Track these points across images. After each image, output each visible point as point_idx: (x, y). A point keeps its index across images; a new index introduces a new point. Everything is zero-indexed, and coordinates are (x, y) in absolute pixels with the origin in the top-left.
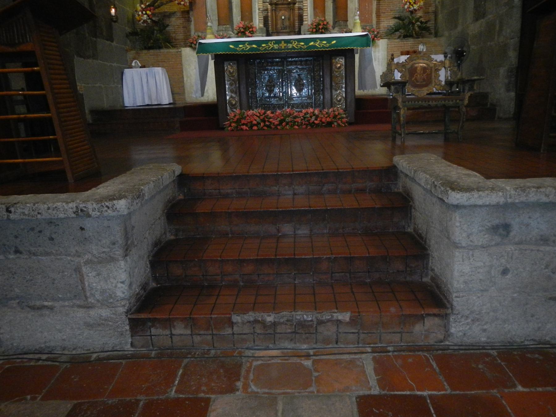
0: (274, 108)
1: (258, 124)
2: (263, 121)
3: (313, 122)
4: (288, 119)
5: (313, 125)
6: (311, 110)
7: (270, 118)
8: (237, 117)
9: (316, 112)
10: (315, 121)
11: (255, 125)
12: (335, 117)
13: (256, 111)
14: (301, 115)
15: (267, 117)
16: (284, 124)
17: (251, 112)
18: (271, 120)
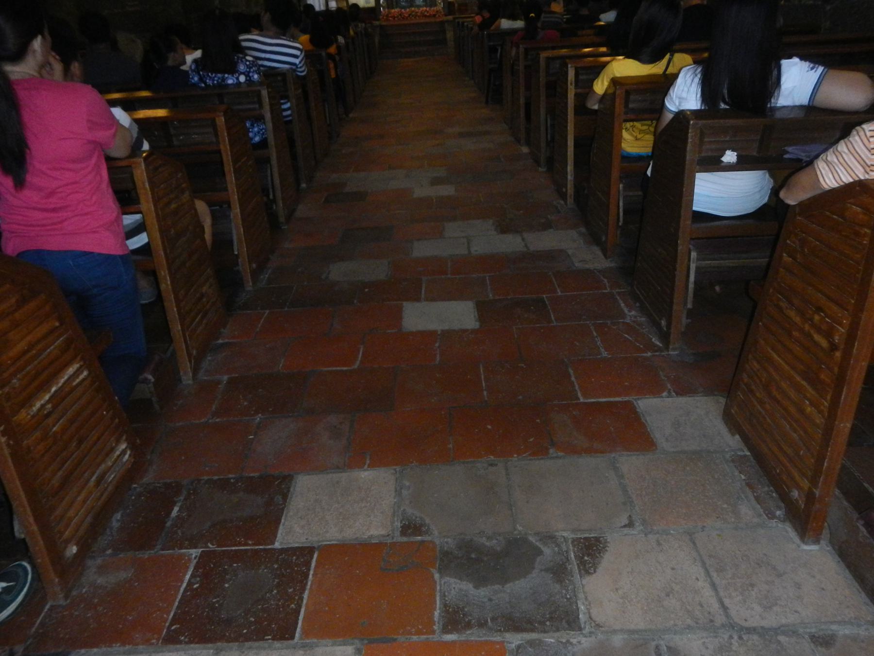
0: (404, 7)
1: (397, 17)
2: (400, 15)
3: (426, 15)
4: (413, 13)
5: (426, 16)
6: (425, 8)
7: (404, 13)
8: (387, 13)
9: (428, 9)
10: (428, 14)
11: (396, 17)
12: (437, 12)
13: (397, 10)
14: (420, 11)
15: (402, 12)
16: (411, 16)
17: (393, 11)
18: (404, 14)
